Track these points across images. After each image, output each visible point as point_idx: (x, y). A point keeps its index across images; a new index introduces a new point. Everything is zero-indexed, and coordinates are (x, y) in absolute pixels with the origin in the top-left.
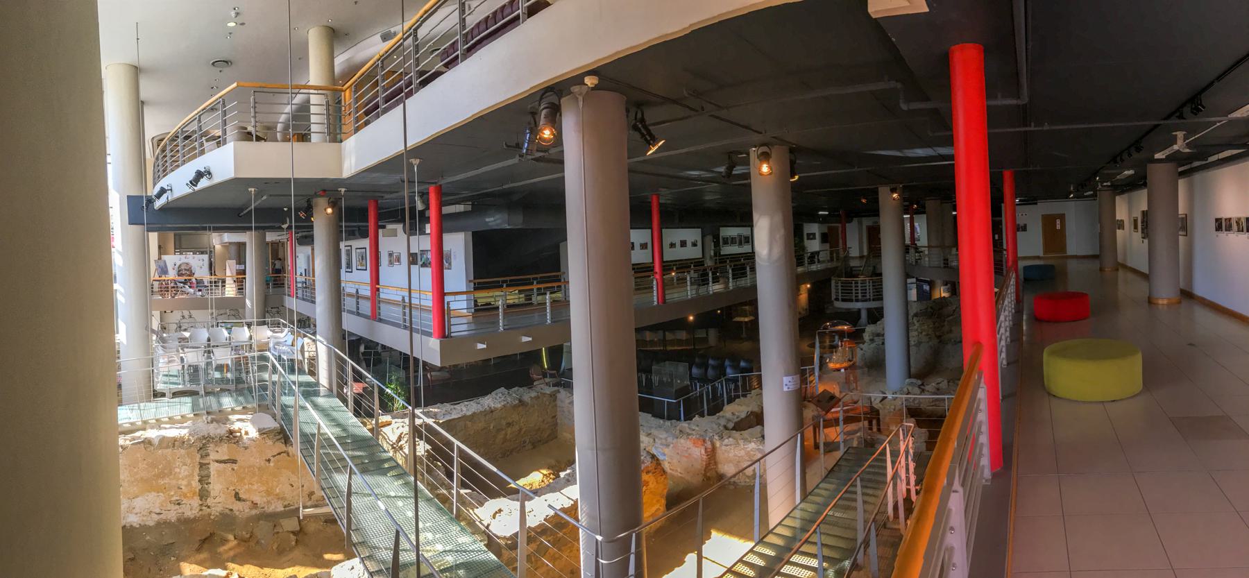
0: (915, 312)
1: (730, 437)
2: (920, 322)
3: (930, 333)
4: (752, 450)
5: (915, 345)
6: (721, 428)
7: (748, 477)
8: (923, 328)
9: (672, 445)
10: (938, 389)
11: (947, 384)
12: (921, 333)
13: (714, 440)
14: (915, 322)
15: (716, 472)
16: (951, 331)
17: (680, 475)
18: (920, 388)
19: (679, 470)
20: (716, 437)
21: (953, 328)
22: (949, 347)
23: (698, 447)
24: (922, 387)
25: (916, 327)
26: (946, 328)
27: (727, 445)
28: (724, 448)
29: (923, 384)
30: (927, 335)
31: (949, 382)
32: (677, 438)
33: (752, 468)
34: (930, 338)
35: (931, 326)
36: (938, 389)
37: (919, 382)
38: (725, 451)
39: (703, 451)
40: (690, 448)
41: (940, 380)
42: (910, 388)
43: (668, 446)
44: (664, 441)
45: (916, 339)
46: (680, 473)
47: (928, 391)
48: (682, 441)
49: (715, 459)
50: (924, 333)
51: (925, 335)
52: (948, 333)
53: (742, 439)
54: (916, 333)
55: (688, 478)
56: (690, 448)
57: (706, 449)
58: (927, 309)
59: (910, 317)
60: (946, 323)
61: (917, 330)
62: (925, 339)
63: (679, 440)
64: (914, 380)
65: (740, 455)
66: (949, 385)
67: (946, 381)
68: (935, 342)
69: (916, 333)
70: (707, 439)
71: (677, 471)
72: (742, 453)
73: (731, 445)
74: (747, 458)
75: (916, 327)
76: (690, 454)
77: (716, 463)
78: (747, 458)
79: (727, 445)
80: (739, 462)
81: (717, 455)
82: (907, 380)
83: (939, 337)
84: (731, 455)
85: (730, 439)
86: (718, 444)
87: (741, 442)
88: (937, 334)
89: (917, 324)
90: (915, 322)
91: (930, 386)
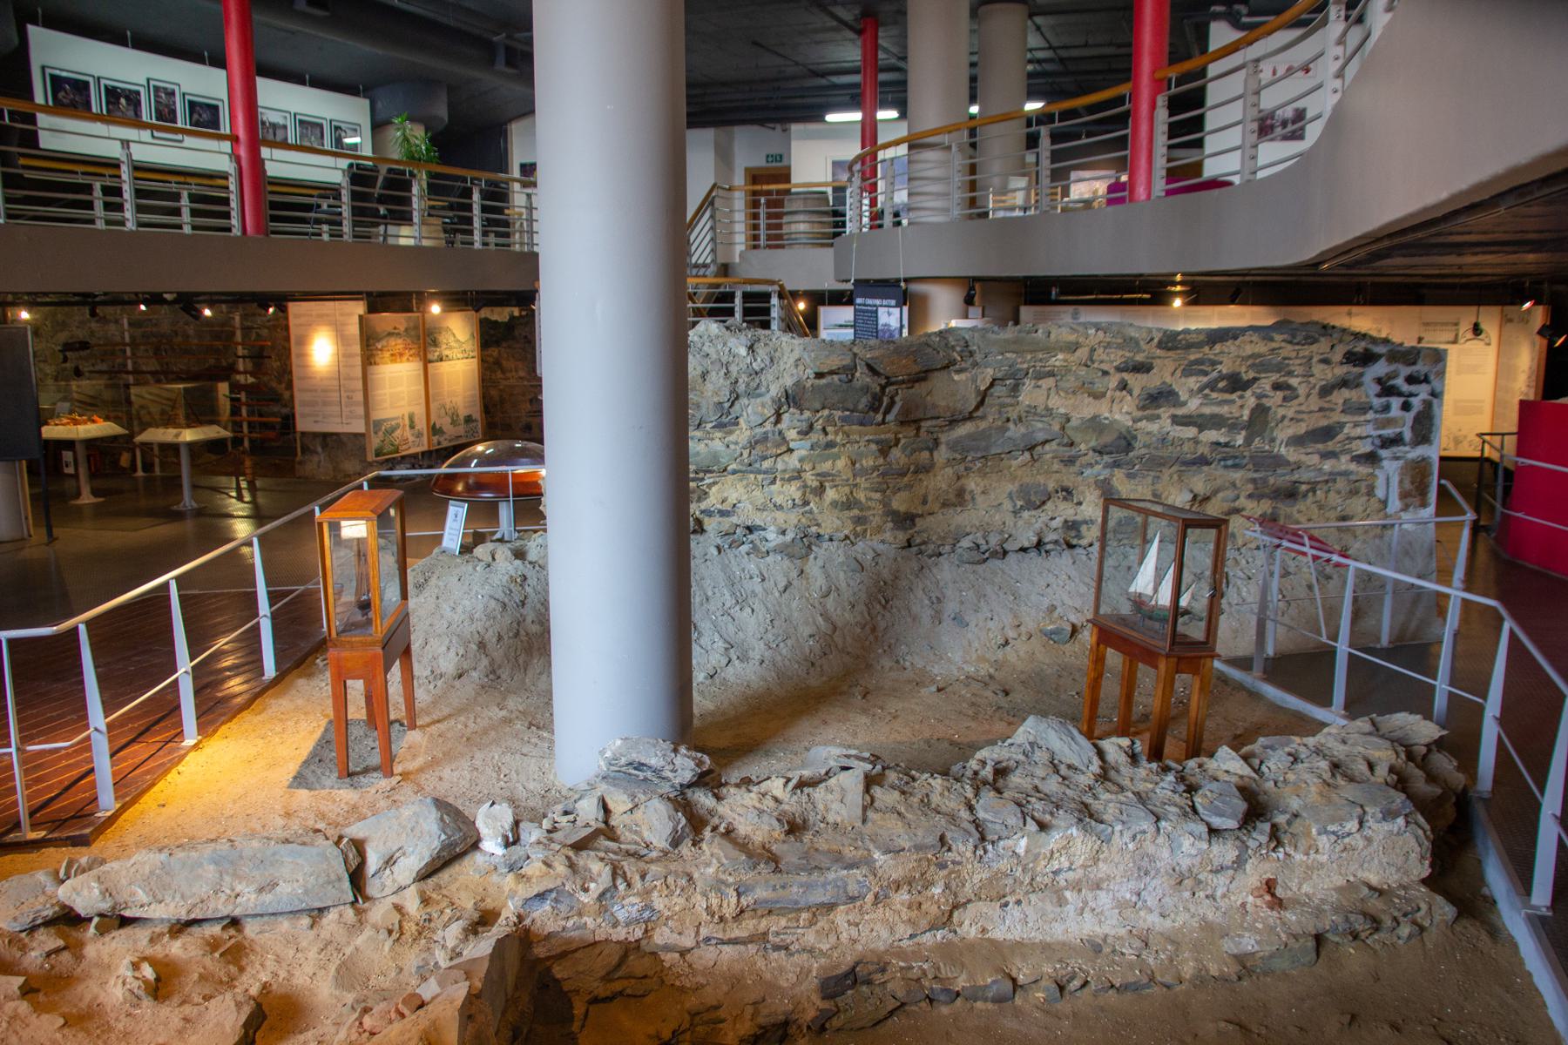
0: (789, 382)
2: (816, 437)
3: (861, 496)
5: (782, 550)
8: (826, 466)
12: (820, 491)
14: (792, 434)
16: (960, 498)
21: (973, 484)
22: (946, 571)
25: (793, 461)
26: (940, 481)
30: (848, 504)
34: (859, 521)
35: (868, 462)
45: (793, 518)
50: (831, 494)
51: (834, 504)
54: (793, 490)
58: (850, 370)
60: (942, 454)
61: (798, 475)
62: (831, 522)
68: (882, 542)
75: (793, 461)
83: (905, 520)
88: (899, 503)
89: (802, 448)
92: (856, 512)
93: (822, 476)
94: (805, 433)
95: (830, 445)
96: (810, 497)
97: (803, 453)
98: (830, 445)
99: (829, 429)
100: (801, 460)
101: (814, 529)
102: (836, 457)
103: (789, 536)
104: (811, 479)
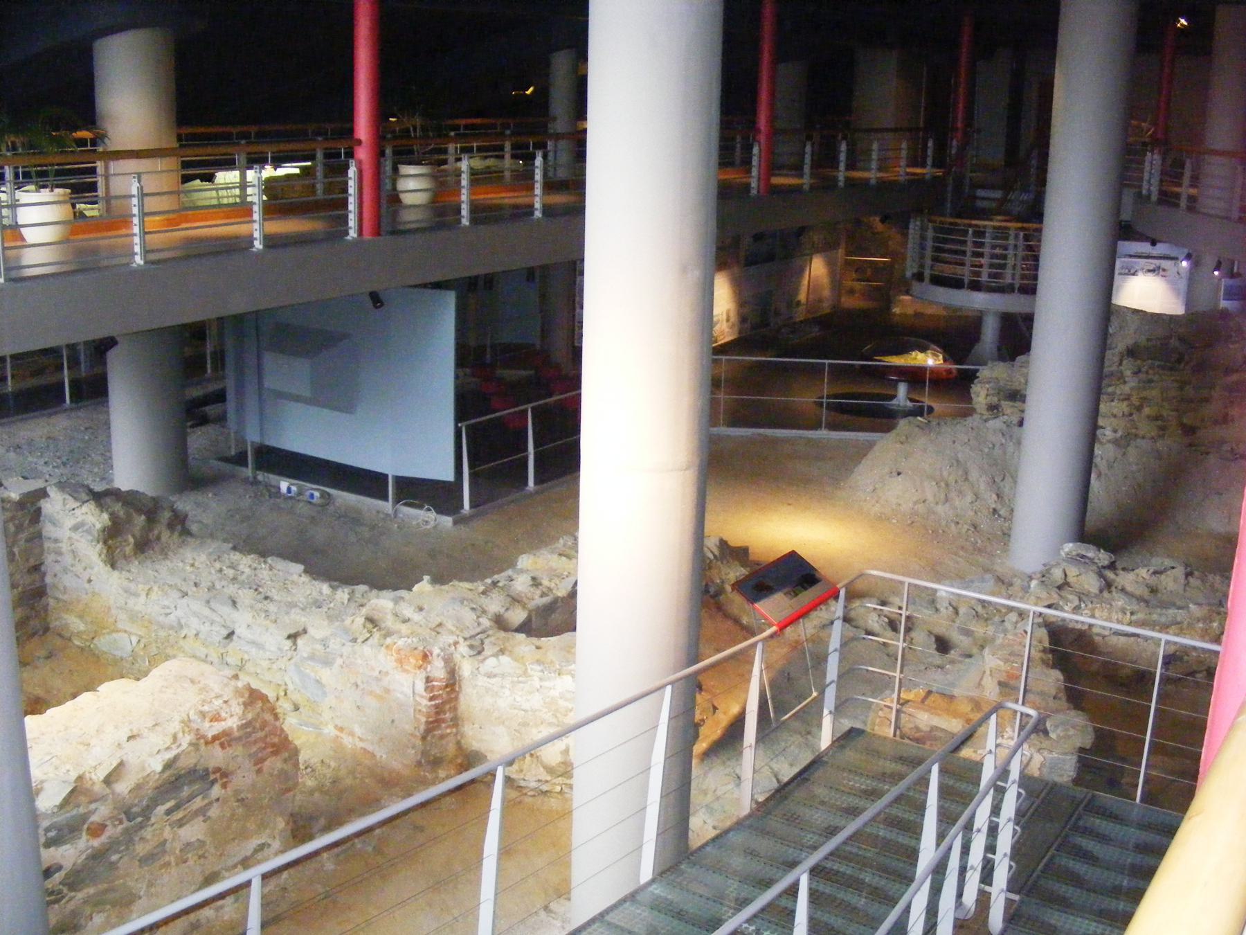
1: (502, 651)
2: (1142, 376)
4: (562, 696)
6: (486, 622)
7: (550, 770)
8: (1145, 394)
9: (339, 661)
10: (1153, 590)
11: (1182, 580)
12: (1139, 409)
13: (457, 657)
14: (1128, 373)
15: (458, 743)
17: (360, 745)
18: (1101, 576)
19: (358, 731)
20: (463, 648)
23: (406, 671)
24: (1110, 574)
25: (1126, 389)
27: (490, 676)
28: (482, 681)
29: (1112, 566)
30: (1156, 418)
31: (1188, 575)
32: (355, 640)
33: (560, 745)
34: (1163, 428)
35: (1172, 393)
36: (1153, 590)
37: (1103, 557)
38: (487, 690)
39: (420, 686)
40: (387, 673)
41: (1158, 562)
42: (1073, 572)
43: (327, 662)
44: (319, 647)
46: (361, 739)
47: (1123, 590)
48: (367, 650)
49: (455, 709)
50: (1147, 411)
51: (1148, 417)
52: (1216, 422)
53: (539, 662)
54: (1124, 407)
55: (382, 754)
56: (387, 673)
57: (428, 680)
59: (1112, 357)
61: (1127, 398)
62: (1145, 428)
63: (357, 647)
64: (1091, 552)
65: (526, 706)
66: (1187, 584)
67: (1180, 572)
69: (1124, 407)
70: (436, 651)
71: (352, 734)
72: (536, 701)
73: (503, 676)
74: (548, 717)
75: (1126, 389)
76: (387, 691)
77: (456, 722)
78: (548, 717)
79: (490, 676)
80: (525, 724)
81: (462, 698)
82: (1069, 547)
83: (1189, 431)
84: (503, 703)
85: (504, 659)
86: (466, 668)
87: (534, 671)
89: (1132, 383)
90: (1128, 373)
91: (1131, 576)
92: (1159, 423)
93: (1144, 399)
94: (1136, 373)
95: (1150, 381)
96: (1135, 411)
97: (1133, 384)
98: (1150, 381)
99: (1151, 372)
100: (1132, 389)
101: (1134, 431)
102: (1153, 388)
103: (1119, 434)
104: (1136, 402)
